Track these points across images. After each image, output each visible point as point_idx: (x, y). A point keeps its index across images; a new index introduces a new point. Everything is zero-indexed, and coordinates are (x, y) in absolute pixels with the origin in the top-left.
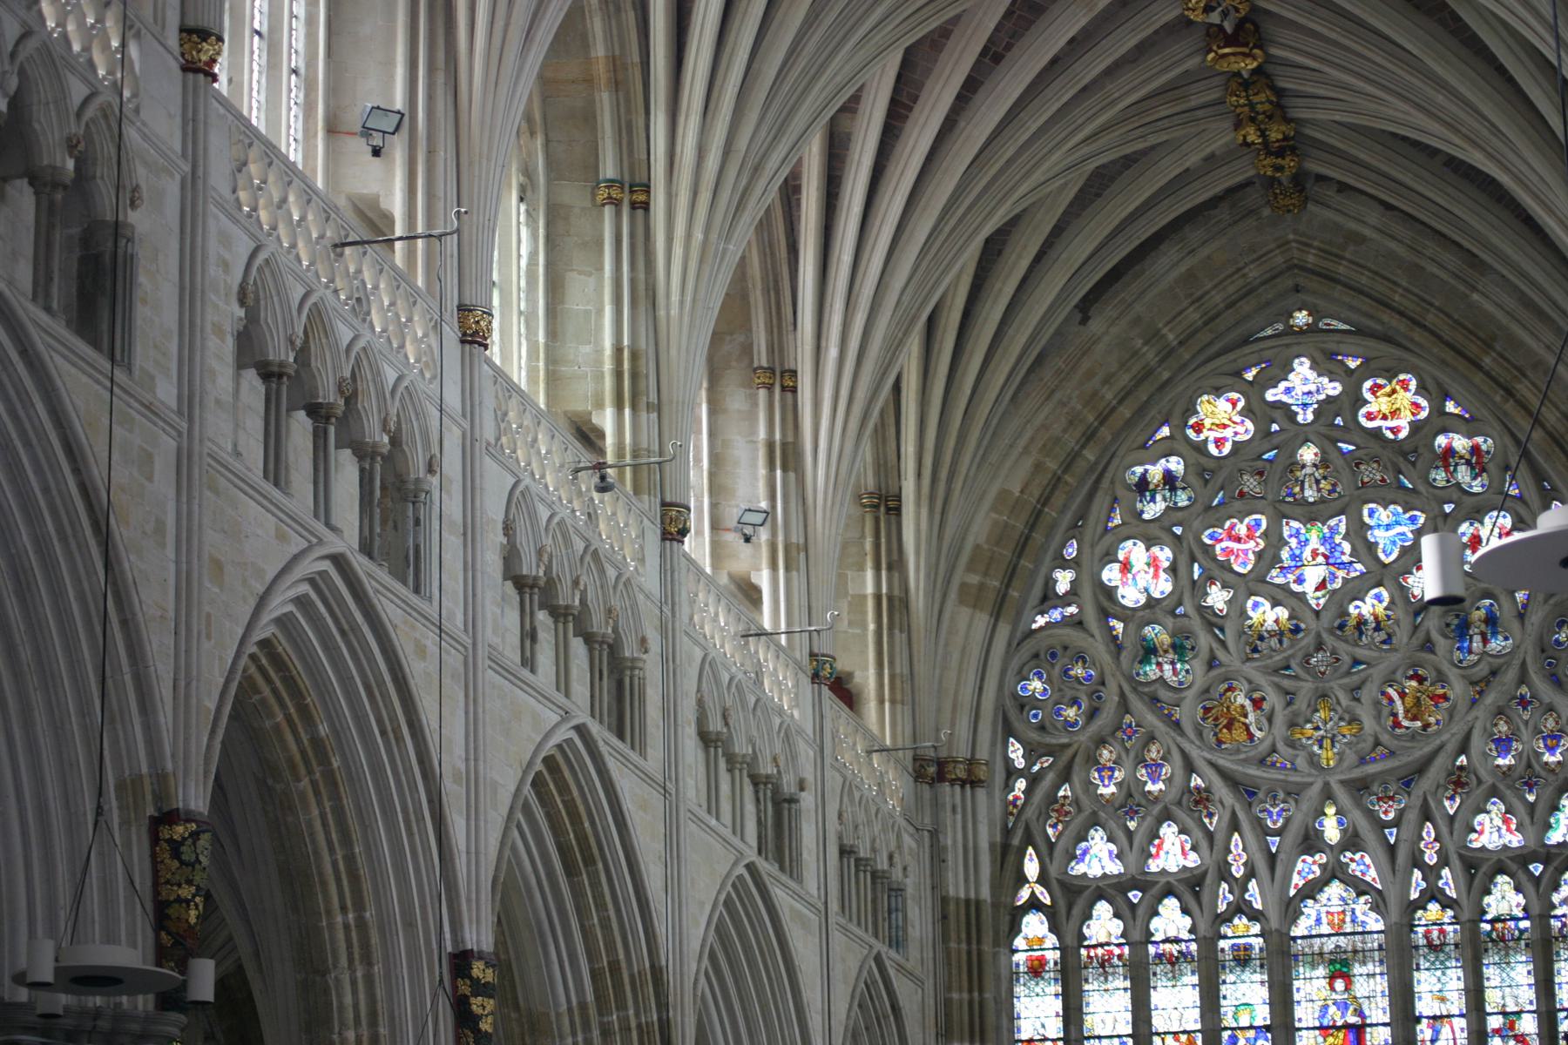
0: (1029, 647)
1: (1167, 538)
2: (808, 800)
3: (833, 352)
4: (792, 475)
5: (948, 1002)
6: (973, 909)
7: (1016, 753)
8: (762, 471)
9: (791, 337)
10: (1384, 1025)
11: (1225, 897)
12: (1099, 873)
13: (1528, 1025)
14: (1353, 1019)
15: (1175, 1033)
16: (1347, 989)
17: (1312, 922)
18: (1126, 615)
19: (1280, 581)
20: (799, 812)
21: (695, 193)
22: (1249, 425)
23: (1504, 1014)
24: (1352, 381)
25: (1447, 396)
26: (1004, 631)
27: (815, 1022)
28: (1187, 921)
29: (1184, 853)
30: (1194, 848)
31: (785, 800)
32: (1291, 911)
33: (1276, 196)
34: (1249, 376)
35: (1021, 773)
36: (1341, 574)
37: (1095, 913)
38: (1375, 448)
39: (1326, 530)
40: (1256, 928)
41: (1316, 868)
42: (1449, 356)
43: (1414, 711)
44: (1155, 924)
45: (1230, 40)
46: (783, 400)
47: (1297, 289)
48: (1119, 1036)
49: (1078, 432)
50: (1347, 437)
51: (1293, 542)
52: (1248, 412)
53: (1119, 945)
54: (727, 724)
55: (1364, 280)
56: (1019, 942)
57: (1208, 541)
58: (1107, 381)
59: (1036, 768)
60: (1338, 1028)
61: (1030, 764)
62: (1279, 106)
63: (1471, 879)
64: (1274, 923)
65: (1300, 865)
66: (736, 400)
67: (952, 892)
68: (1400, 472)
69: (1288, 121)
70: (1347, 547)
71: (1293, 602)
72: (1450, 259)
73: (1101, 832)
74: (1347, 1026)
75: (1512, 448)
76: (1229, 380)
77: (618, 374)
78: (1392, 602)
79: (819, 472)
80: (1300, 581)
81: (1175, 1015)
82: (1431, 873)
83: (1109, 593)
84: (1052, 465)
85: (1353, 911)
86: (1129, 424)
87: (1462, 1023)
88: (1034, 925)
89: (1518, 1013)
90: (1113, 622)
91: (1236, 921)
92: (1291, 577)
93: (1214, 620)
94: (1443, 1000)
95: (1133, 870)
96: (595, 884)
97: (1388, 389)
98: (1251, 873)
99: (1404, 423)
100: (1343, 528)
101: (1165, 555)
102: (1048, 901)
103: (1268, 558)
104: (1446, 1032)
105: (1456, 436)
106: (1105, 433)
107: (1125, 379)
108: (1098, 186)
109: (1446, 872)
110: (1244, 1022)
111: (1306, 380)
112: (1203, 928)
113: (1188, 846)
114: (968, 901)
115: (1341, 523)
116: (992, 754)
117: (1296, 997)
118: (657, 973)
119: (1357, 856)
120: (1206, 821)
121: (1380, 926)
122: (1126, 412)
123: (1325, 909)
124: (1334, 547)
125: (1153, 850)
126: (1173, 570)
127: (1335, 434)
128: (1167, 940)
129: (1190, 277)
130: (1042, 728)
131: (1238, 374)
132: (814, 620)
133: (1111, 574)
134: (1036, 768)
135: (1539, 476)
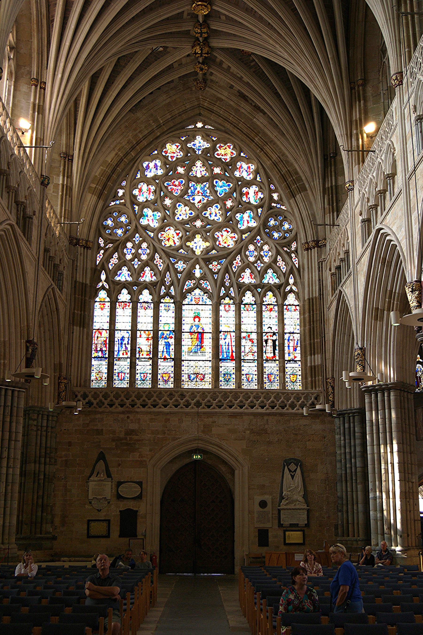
1: (154, 183)
2: (35, 221)
3: (60, 76)
4: (41, 115)
5: (74, 314)
6: (84, 286)
7: (101, 242)
8: (31, 112)
9: (45, 72)
10: (210, 333)
11: (163, 291)
12: (125, 280)
13: (254, 336)
14: (200, 330)
16: (199, 321)
17: (190, 300)
18: (138, 204)
19: (188, 199)
20: (32, 222)
22: (181, 153)
23: (247, 332)
24: (214, 144)
27: (31, 296)
29: (152, 277)
30: (155, 275)
31: (28, 217)
32: (184, 297)
33: (197, 83)
34: (183, 139)
35: (102, 248)
36: (206, 199)
37: (122, 292)
39: (202, 186)
40: (172, 301)
41: (192, 284)
42: (244, 138)
43: (225, 241)
44: (140, 297)
46: (40, 91)
47: (200, 114)
50: (211, 159)
51: (192, 188)
52: (181, 149)
53: (129, 302)
54: (9, 168)
56: (97, 299)
57: (166, 185)
59: (107, 247)
61: (106, 246)
64: (178, 299)
65: (187, 283)
66: (24, 88)
67: (78, 280)
68: (226, 171)
69: (210, 47)
70: (208, 191)
71: (191, 205)
72: (248, 108)
73: (126, 268)
74: (199, 333)
75: (260, 166)
76: (177, 139)
78: (221, 208)
80: (193, 199)
82: (227, 289)
83: (135, 197)
86: (146, 147)
87: (233, 334)
88: (103, 294)
90: (135, 206)
91: (166, 298)
92: (191, 198)
93: (166, 207)
95: (135, 280)
97: (224, 148)
98: (172, 284)
99: (228, 157)
100: (207, 186)
101: (153, 188)
102: (108, 287)
104: (229, 336)
105: (243, 163)
107: (146, 132)
109: (232, 289)
111: (200, 142)
112: (156, 299)
113: (153, 274)
114: (83, 283)
116: (94, 240)
117: (183, 322)
119: (205, 282)
120: (159, 267)
121: (211, 303)
122: (145, 143)
123: (193, 297)
124: (204, 191)
125: (142, 275)
127: (208, 158)
128: (144, 302)
130: (110, 234)
132: (45, 144)
133: (136, 192)
134: (107, 247)
135: (268, 177)
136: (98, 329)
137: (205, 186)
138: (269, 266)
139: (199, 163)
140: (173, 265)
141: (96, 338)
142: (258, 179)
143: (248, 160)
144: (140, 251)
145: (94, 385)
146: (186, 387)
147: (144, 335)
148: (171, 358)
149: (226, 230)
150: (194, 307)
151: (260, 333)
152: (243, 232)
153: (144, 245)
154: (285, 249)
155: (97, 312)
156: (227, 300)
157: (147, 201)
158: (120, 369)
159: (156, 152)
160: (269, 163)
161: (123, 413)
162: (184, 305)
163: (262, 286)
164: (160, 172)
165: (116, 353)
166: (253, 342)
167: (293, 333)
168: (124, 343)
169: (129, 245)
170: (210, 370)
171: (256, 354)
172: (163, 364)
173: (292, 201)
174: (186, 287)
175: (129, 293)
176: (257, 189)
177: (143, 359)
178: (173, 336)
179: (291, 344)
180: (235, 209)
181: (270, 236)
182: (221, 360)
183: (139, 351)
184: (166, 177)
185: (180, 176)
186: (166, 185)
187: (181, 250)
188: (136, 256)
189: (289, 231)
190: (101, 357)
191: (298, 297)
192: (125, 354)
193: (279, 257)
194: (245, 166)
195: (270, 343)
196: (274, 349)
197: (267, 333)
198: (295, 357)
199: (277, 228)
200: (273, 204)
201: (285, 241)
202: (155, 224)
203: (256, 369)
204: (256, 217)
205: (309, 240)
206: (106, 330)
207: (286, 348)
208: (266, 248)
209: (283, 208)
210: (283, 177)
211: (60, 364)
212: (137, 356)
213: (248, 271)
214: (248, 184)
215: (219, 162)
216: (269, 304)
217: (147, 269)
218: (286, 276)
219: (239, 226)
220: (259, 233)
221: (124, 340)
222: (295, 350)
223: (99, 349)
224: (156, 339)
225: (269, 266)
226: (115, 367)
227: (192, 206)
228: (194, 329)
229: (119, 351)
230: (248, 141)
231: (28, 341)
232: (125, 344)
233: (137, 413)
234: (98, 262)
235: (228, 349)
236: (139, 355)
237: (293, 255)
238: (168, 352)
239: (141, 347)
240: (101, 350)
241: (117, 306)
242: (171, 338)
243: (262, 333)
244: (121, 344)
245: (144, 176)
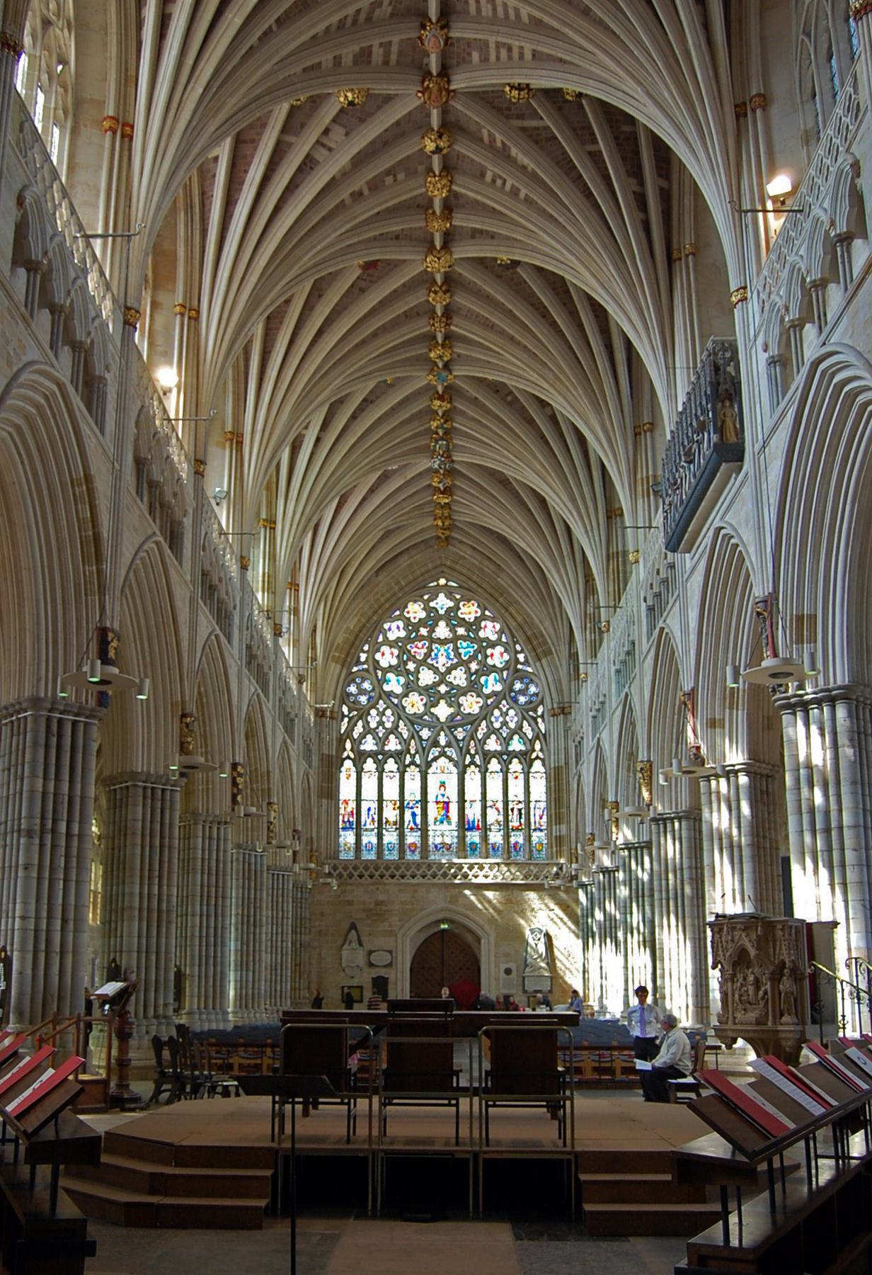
0: (352, 676)
3: (312, 580)
7: (345, 709)
13: (500, 805)
14: (446, 800)
18: (382, 669)
21: (291, 526)
24: (457, 602)
25: (486, 609)
26: (344, 671)
28: (396, 766)
32: (429, 765)
36: (450, 662)
38: (463, 623)
42: (489, 597)
44: (386, 766)
45: (443, 493)
49: (372, 611)
52: (424, 609)
55: (464, 571)
56: (343, 769)
58: (382, 595)
62: (450, 515)
63: (485, 759)
64: (424, 769)
70: (452, 654)
72: (492, 567)
77: (264, 581)
79: (305, 616)
82: (473, 757)
83: (378, 662)
84: (363, 620)
86: (388, 609)
88: (348, 764)
92: (434, 662)
96: (254, 743)
103: (428, 655)
106: (380, 612)
107: (388, 595)
108: (387, 534)
109: (477, 756)
115: (451, 646)
118: (268, 772)
122: (387, 606)
124: (448, 654)
126: (398, 656)
129: (410, 565)
130: (353, 702)
131: (422, 597)
133: (378, 656)
135: (513, 636)
138: (514, 732)
139: (442, 624)
140: (418, 732)
142: (504, 639)
143: (493, 620)
144: (384, 719)
145: (343, 856)
146: (433, 857)
147: (391, 806)
151: (506, 802)
152: (488, 697)
153: (389, 712)
154: (531, 713)
157: (390, 666)
159: (398, 613)
160: (514, 624)
161: (373, 884)
163: (509, 753)
164: (403, 634)
169: (373, 712)
170: (456, 840)
173: (538, 664)
176: (503, 650)
179: (538, 812)
180: (480, 673)
181: (515, 700)
184: (408, 640)
185: (422, 638)
186: (408, 647)
187: (426, 717)
188: (381, 723)
189: (537, 695)
191: (544, 765)
193: (525, 723)
194: (489, 624)
195: (516, 812)
196: (520, 818)
199: (523, 692)
200: (519, 666)
201: (531, 706)
202: (398, 690)
204: (502, 680)
205: (555, 706)
207: (532, 817)
208: (512, 712)
209: (530, 669)
210: (528, 638)
211: (312, 838)
213: (494, 737)
214: (493, 645)
215: (463, 622)
217: (392, 737)
218: (532, 742)
219: (484, 689)
220: (504, 698)
222: (541, 818)
223: (346, 819)
224: (402, 809)
225: (515, 733)
226: (363, 838)
227: (436, 670)
228: (440, 799)
230: (492, 600)
231: (294, 831)
233: (386, 884)
234: (342, 731)
237: (539, 720)
243: (507, 801)
245: (386, 638)
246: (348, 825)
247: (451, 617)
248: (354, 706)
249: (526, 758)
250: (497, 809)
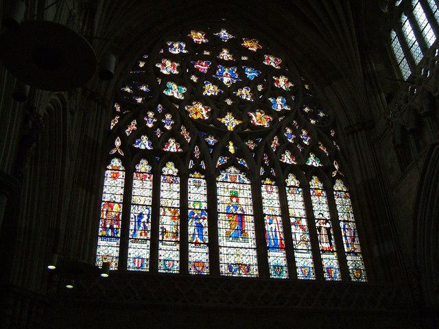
13: (304, 222)
14: (240, 212)
15: (169, 207)
35: (118, 114)
40: (203, 177)
48: (147, 206)
51: (220, 70)
56: (110, 167)
60: (234, 214)
65: (220, 159)
74: (237, 214)
81: (170, 201)
85: (239, 176)
87: (279, 219)
88: (116, 162)
89: (301, 218)
94: (273, 210)
98: (202, 157)
100: (236, 70)
104: (275, 220)
110: (197, 207)
111: (225, 34)
136: (108, 202)
137: (233, 70)
141: (105, 213)
148: (204, 243)
149: (259, 112)
150: (231, 186)
153: (168, 116)
155: (108, 181)
156: (268, 181)
158: (137, 253)
162: (218, 181)
165: (131, 233)
166: (304, 230)
167: (348, 221)
168: (142, 220)
170: (255, 261)
171: (309, 243)
172: (193, 250)
174: (218, 163)
175: (149, 164)
177: (167, 243)
178: (206, 217)
182: (269, 248)
183: (163, 232)
190: (111, 237)
192: (143, 234)
195: (323, 231)
196: (330, 239)
197: (318, 219)
198: (355, 249)
203: (311, 260)
206: (118, 203)
212: (160, 238)
216: (316, 189)
217: (172, 141)
221: (142, 218)
222: (353, 240)
223: (108, 226)
226: (130, 251)
229: (135, 230)
232: (144, 222)
234: (112, 127)
235: (276, 236)
236: (163, 238)
238: (201, 236)
239: (165, 226)
240: (111, 227)
241: (135, 176)
242: (204, 219)
244: (139, 221)
246: (110, 233)
247: (234, 46)
248: (128, 103)
249: (324, 174)
250: (302, 227)
